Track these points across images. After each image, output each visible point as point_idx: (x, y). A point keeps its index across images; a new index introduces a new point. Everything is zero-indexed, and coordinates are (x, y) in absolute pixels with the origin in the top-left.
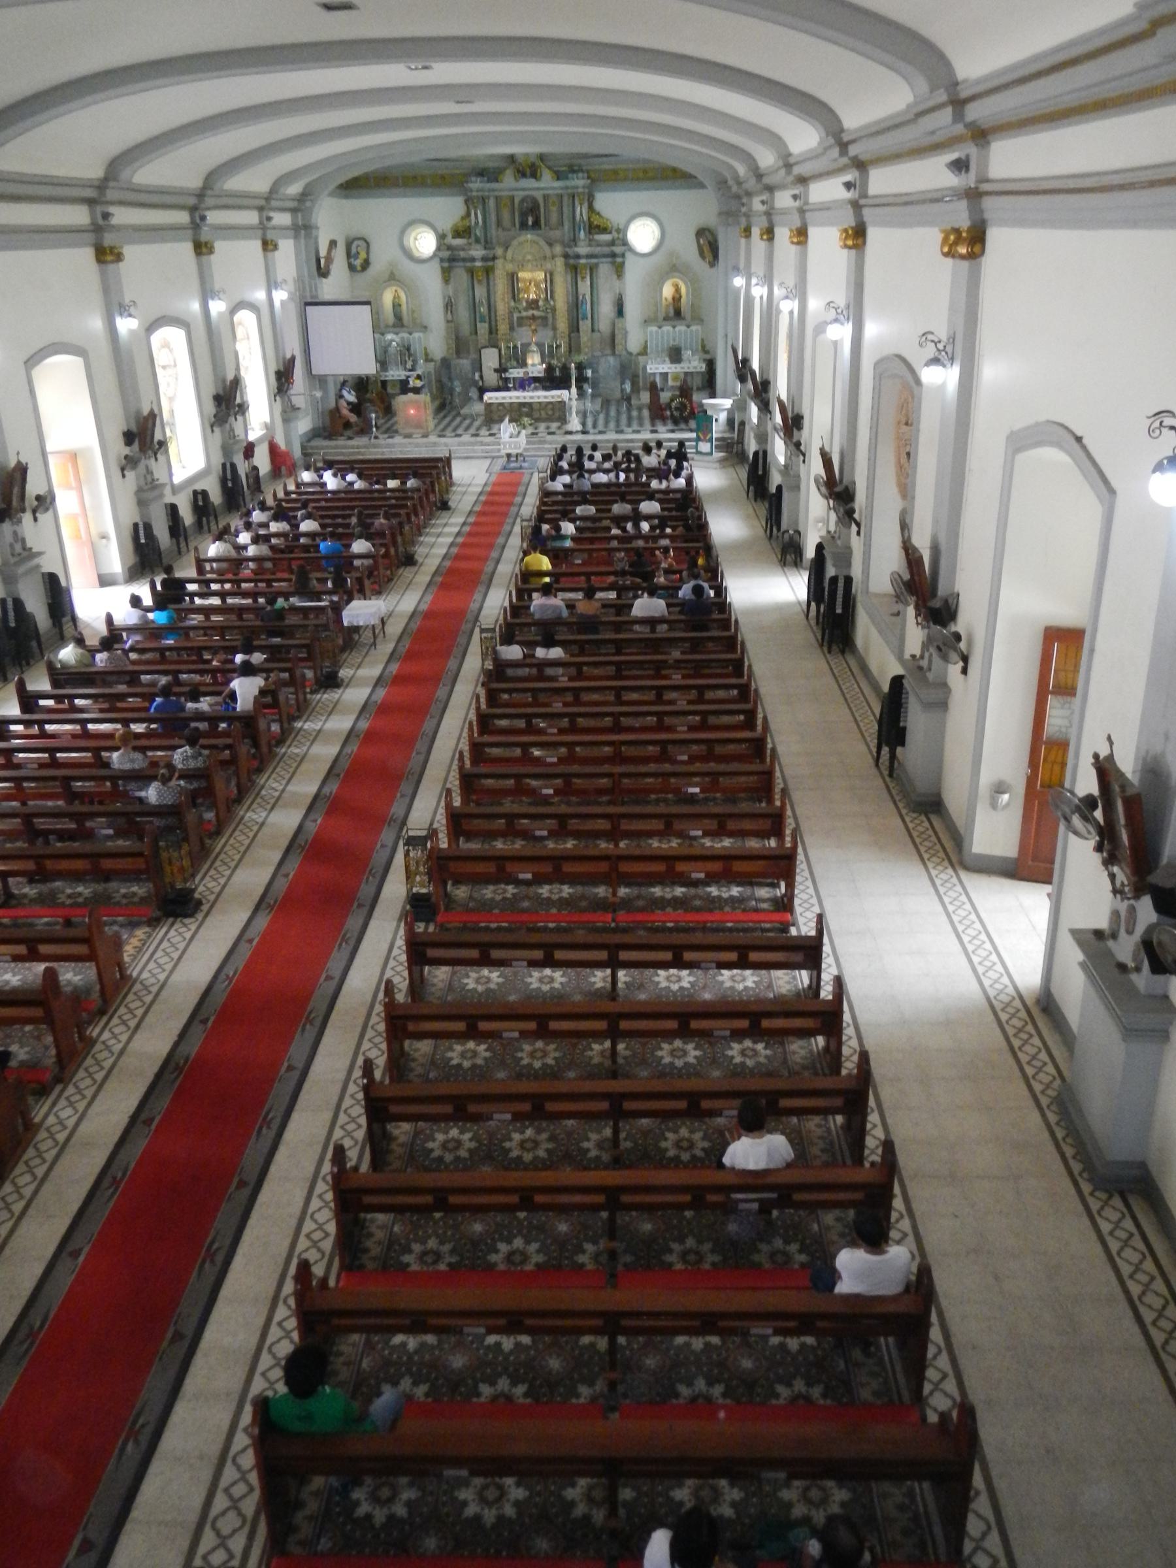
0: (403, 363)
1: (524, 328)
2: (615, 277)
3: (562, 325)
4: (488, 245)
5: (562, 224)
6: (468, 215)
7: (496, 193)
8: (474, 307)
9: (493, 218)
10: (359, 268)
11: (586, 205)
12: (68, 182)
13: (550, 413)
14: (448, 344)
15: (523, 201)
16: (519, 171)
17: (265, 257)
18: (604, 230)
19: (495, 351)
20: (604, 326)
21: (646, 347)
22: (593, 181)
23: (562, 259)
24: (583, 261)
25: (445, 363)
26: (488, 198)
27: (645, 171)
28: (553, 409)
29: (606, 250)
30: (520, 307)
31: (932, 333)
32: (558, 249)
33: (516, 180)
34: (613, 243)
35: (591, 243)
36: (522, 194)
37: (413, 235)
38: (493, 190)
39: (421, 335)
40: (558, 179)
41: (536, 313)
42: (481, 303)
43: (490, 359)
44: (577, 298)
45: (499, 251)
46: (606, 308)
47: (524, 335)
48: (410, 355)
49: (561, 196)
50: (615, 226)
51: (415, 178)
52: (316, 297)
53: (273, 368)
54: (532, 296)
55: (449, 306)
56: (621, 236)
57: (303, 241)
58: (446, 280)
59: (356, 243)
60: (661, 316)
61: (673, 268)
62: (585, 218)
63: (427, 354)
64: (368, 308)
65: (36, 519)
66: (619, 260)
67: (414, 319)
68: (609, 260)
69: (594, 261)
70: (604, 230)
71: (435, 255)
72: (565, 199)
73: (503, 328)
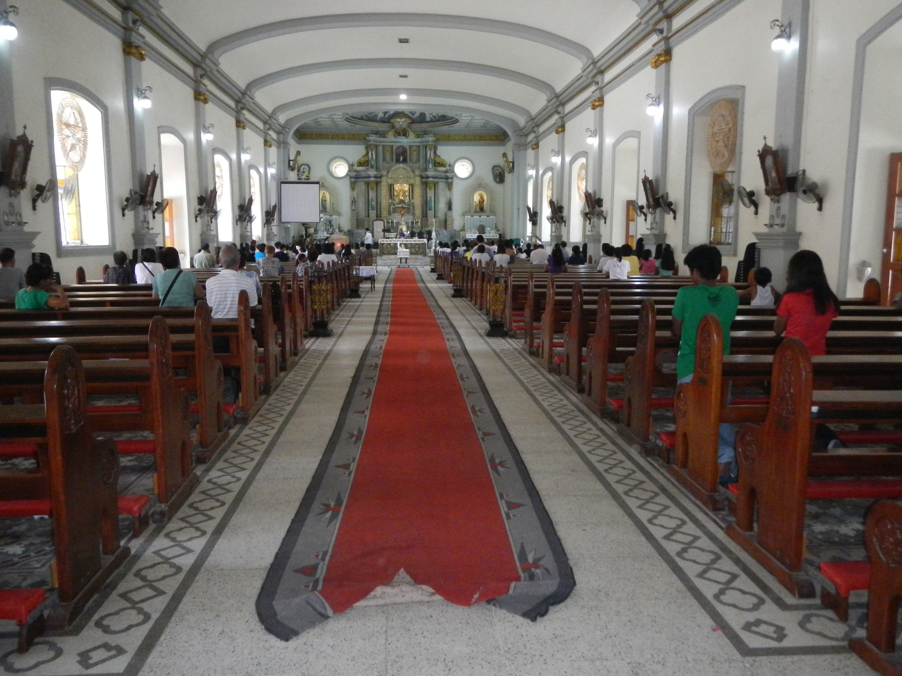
0: (327, 230)
1: (396, 214)
2: (447, 189)
3: (418, 212)
4: (377, 169)
5: (419, 161)
6: (367, 154)
7: (384, 144)
8: (368, 202)
9: (381, 156)
11: (433, 150)
12: (188, 40)
13: (417, 250)
14: (352, 222)
15: (397, 148)
16: (396, 132)
17: (265, 150)
18: (442, 165)
19: (382, 222)
20: (441, 215)
21: (464, 226)
22: (437, 140)
23: (419, 178)
24: (431, 179)
25: (350, 233)
26: (379, 146)
27: (465, 136)
28: (418, 248)
29: (443, 175)
30: (395, 203)
31: (777, 21)
32: (417, 173)
33: (395, 137)
34: (446, 172)
35: (435, 170)
36: (399, 144)
37: (335, 165)
38: (383, 142)
39: (337, 216)
40: (418, 137)
41: (404, 206)
42: (372, 199)
43: (379, 226)
44: (427, 198)
45: (384, 173)
46: (442, 206)
47: (396, 218)
48: (331, 226)
50: (448, 163)
51: (337, 135)
52: (287, 179)
53: (264, 210)
54: (401, 198)
55: (354, 202)
57: (282, 150)
58: (353, 189)
59: (303, 167)
60: (472, 212)
61: (480, 186)
62: (432, 158)
63: (339, 228)
64: (318, 185)
65: (154, 217)
66: (450, 180)
67: (333, 208)
68: (445, 180)
69: (437, 180)
70: (442, 165)
71: (347, 175)
72: (421, 147)
73: (384, 213)
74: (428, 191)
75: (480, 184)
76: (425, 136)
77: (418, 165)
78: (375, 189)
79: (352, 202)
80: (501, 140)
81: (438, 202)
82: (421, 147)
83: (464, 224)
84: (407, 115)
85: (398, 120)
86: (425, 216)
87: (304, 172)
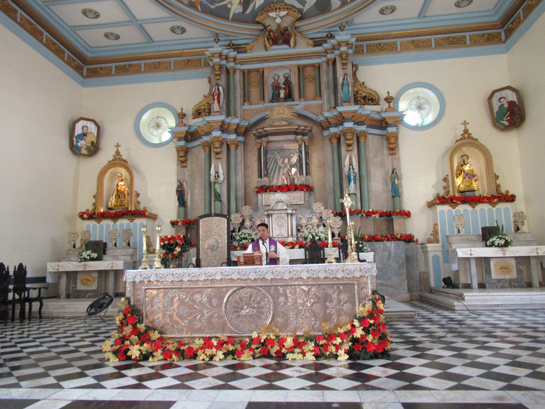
2: (386, 152)
5: (320, 96)
9: (239, 92)
10: (84, 151)
18: (372, 99)
21: (435, 233)
24: (348, 125)
26: (235, 71)
33: (267, 50)
40: (315, 45)
49: (318, 67)
56: (391, 105)
59: (81, 123)
66: (390, 130)
69: (363, 128)
72: (324, 67)
74: (343, 149)
75: (466, 131)
77: (320, 102)
78: (224, 156)
80: (500, 41)
81: (369, 180)
83: (436, 225)
84: (290, 5)
85: (272, 14)
87: (85, 135)
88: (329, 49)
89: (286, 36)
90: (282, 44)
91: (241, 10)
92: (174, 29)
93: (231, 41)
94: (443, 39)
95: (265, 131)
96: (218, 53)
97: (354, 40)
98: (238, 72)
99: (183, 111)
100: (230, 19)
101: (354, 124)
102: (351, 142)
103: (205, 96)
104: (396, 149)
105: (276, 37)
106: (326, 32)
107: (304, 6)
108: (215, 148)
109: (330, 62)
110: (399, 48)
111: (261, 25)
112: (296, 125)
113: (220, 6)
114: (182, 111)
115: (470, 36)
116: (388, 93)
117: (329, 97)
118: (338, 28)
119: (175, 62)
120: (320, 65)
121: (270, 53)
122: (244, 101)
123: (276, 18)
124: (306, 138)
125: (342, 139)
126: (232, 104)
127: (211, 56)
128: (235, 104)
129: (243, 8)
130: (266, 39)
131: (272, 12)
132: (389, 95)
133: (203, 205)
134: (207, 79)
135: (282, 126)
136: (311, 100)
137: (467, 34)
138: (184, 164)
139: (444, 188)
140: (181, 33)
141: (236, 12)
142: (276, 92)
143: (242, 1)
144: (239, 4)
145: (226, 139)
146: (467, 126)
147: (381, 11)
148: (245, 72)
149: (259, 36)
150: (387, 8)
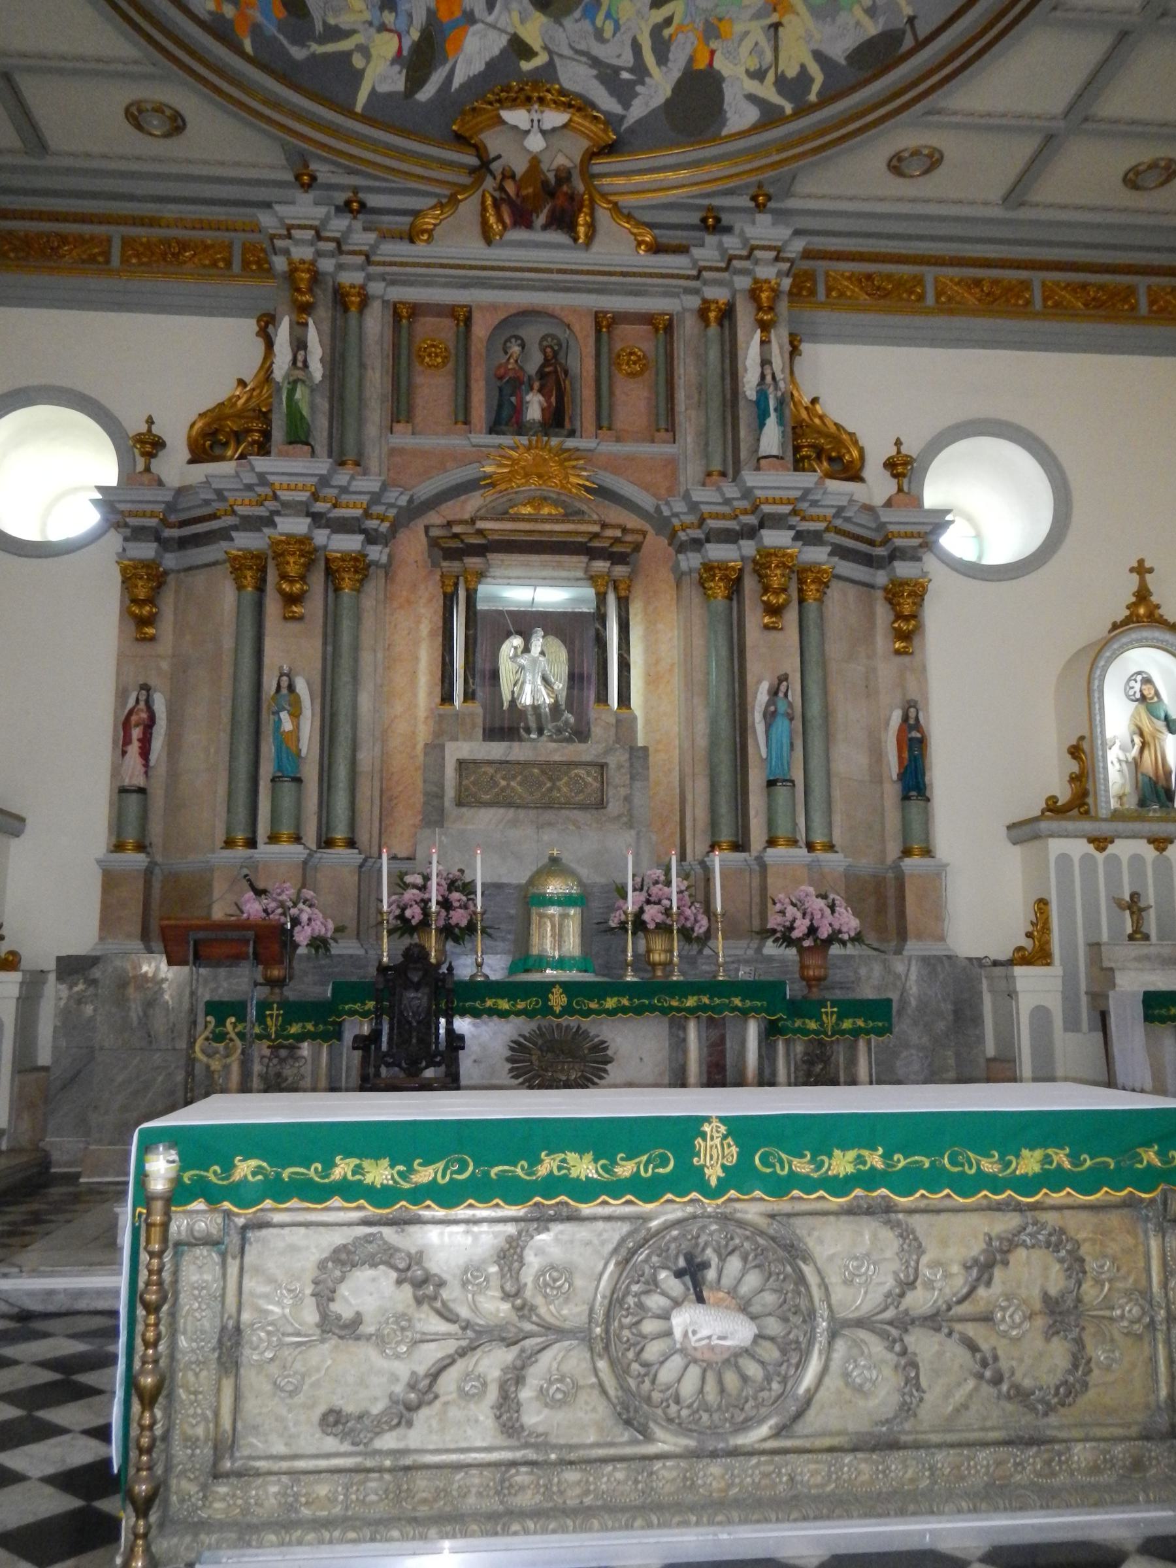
2: (882, 642)
5: (671, 428)
9: (377, 380)
11: (779, 338)
33: (489, 241)
66: (903, 569)
69: (817, 555)
72: (689, 327)
74: (754, 619)
75: (1143, 595)
76: (711, 240)
77: (669, 449)
78: (314, 606)
79: (126, 725)
81: (828, 738)
82: (689, 327)
84: (579, 96)
85: (516, 117)
86: (726, 835)
88: (711, 269)
89: (561, 201)
90: (545, 227)
91: (400, 85)
92: (140, 111)
93: (356, 190)
94: (1071, 287)
95: (480, 532)
96: (310, 227)
97: (797, 246)
98: (375, 308)
99: (155, 430)
100: (359, 108)
101: (795, 539)
102: (782, 598)
103: (242, 383)
104: (916, 641)
105: (525, 199)
106: (698, 208)
107: (626, 105)
108: (284, 577)
109: (712, 315)
110: (930, 300)
111: (473, 152)
112: (595, 522)
113: (326, 56)
114: (149, 430)
115: (1149, 287)
116: (898, 443)
117: (704, 435)
118: (744, 201)
119: (127, 242)
120: (671, 320)
121: (498, 254)
122: (395, 419)
123: (528, 132)
124: (620, 571)
125: (750, 584)
126: (351, 420)
127: (280, 237)
128: (361, 422)
129: (407, 80)
130: (489, 202)
131: (514, 103)
132: (899, 452)
133: (222, 790)
134: (254, 321)
135: (545, 520)
136: (637, 441)
137: (1142, 283)
138: (150, 631)
139: (1074, 779)
140: (167, 135)
141: (383, 88)
142: (513, 399)
143: (405, 53)
144: (394, 62)
145: (325, 547)
146: (1148, 576)
147: (894, 162)
148: (405, 313)
149: (464, 188)
150: (916, 153)
